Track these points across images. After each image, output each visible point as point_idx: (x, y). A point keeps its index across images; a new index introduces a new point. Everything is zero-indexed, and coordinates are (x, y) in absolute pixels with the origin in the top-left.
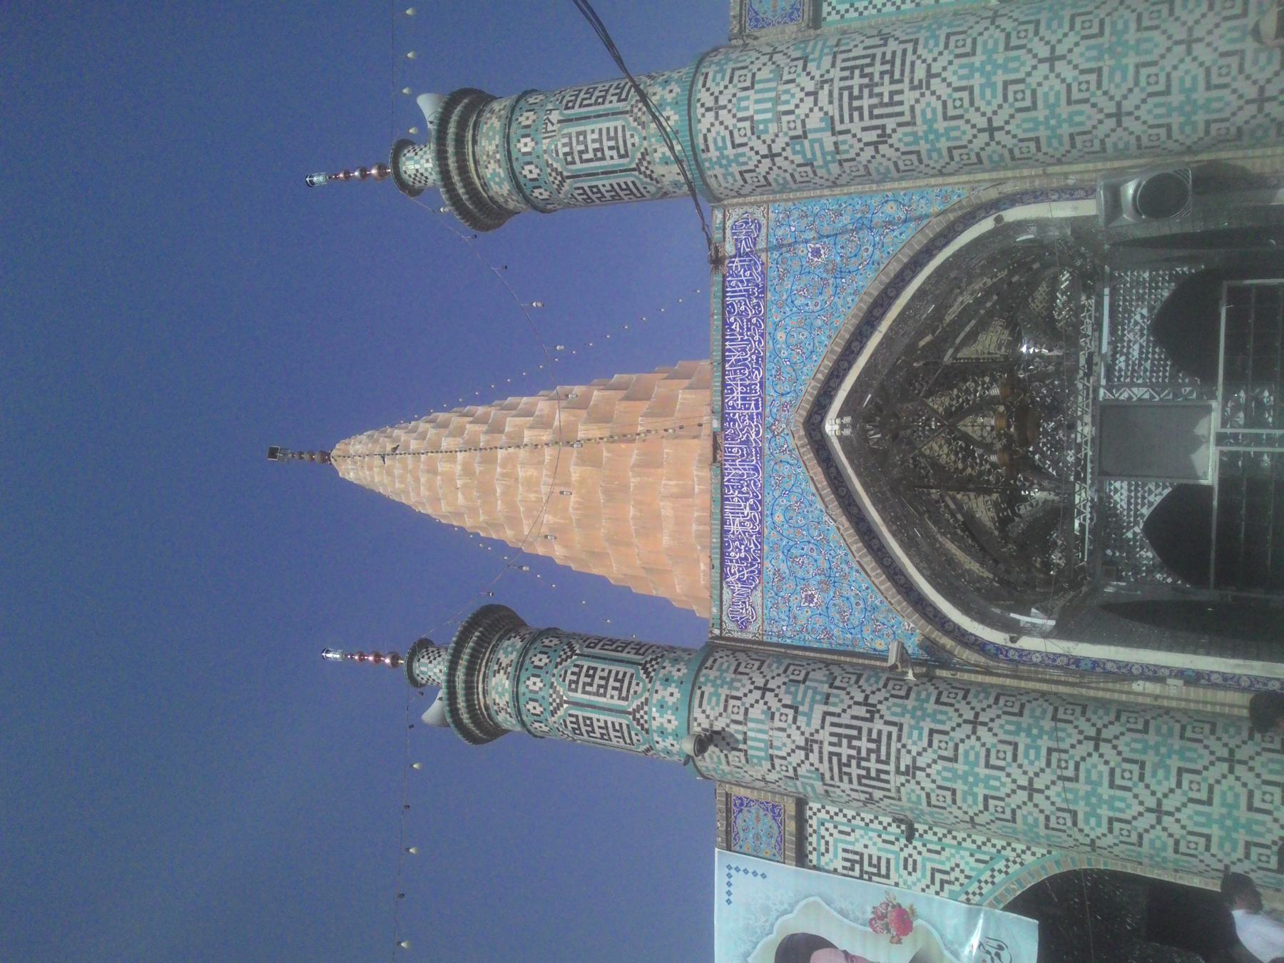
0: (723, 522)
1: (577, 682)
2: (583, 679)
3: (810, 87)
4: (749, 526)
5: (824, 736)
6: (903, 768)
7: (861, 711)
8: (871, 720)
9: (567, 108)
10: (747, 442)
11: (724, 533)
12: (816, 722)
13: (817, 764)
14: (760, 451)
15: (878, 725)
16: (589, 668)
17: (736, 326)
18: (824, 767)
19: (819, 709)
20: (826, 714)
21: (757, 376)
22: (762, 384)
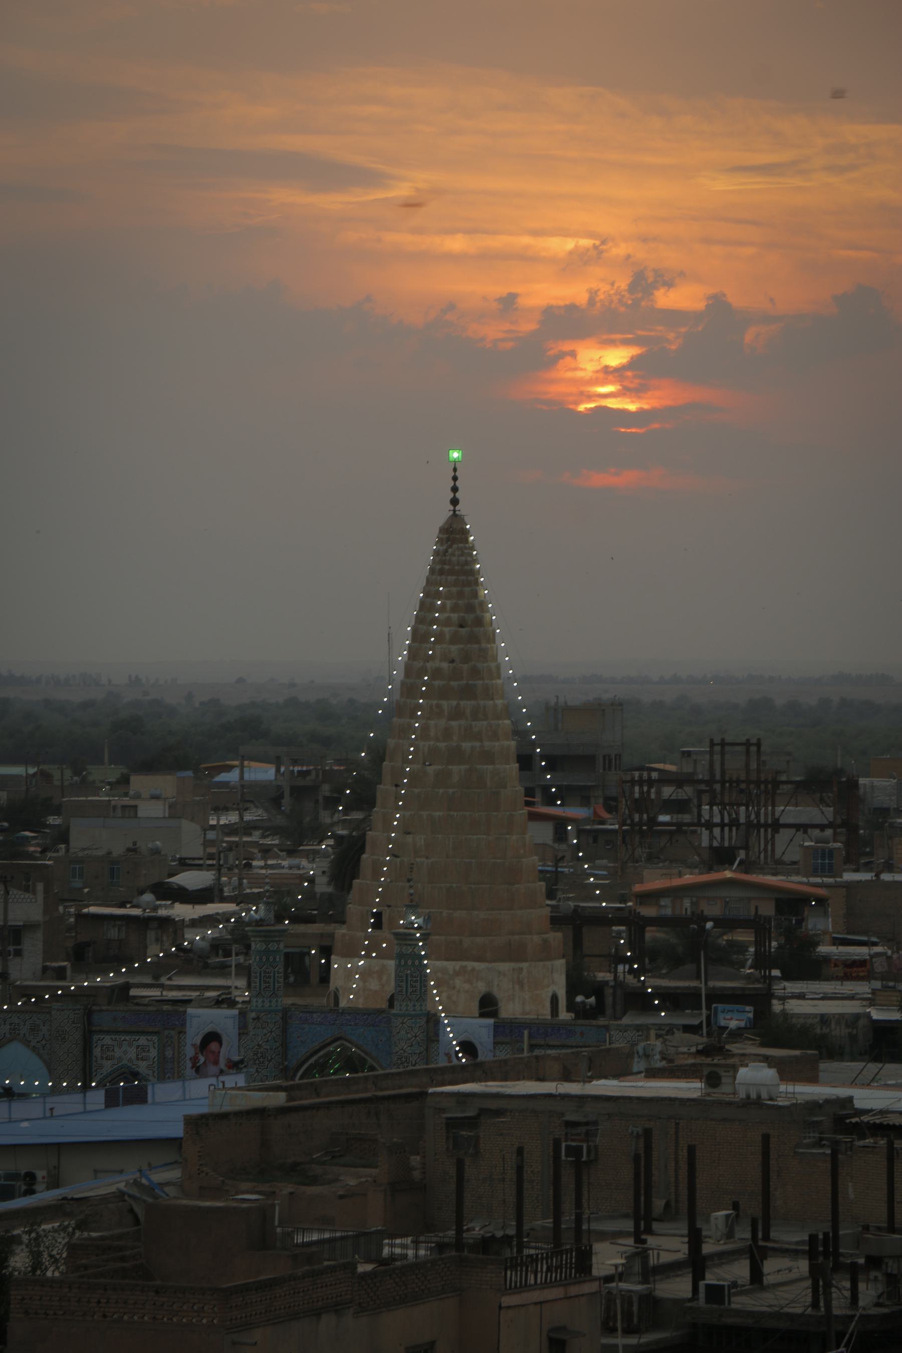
0: (316, 1012)
1: (266, 973)
2: (267, 975)
3: (404, 1048)
4: (315, 1020)
5: (262, 1050)
6: (258, 1069)
7: (269, 1058)
8: (268, 1061)
9: (411, 975)
10: (336, 1020)
11: (313, 1012)
12: (265, 1047)
13: (255, 1048)
14: (333, 1024)
15: (267, 1063)
16: (271, 976)
17: (365, 1017)
18: (254, 1049)
19: (268, 1048)
20: (267, 1049)
21: (353, 1023)
22: (351, 1025)
